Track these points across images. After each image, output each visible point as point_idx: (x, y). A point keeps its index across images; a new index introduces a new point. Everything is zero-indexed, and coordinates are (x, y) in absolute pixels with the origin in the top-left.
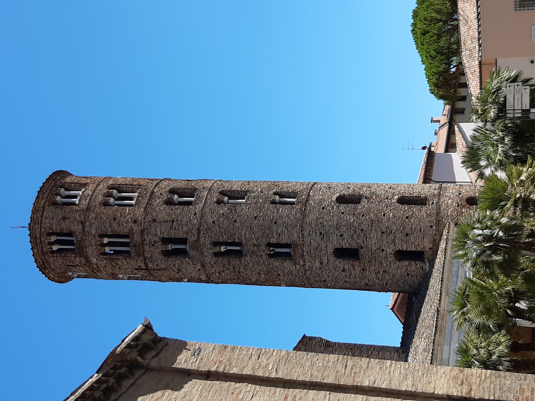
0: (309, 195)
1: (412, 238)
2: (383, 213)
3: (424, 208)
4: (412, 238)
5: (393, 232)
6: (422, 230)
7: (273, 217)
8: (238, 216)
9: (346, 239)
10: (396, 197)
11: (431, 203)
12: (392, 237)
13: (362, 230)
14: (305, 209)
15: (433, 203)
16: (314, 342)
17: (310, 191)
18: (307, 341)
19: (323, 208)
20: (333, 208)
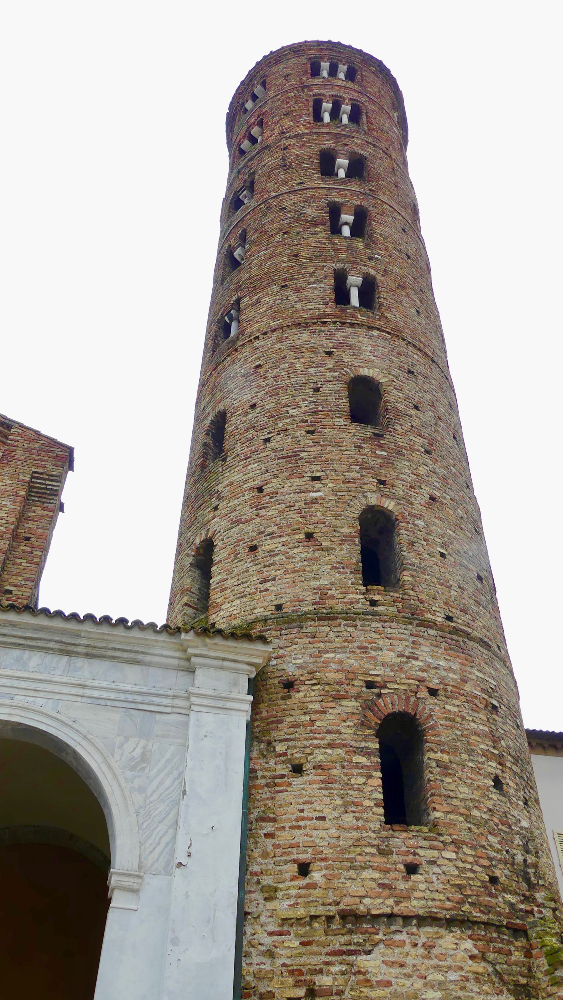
0: (371, 328)
1: (242, 566)
2: (318, 474)
3: (353, 578)
4: (242, 566)
5: (262, 512)
6: (268, 585)
7: (296, 279)
8: (298, 233)
9: (244, 419)
10: (389, 505)
11: (376, 597)
12: (247, 512)
13: (268, 440)
14: (324, 323)
15: (373, 603)
16: (48, 465)
17: (389, 333)
18: (52, 452)
19: (329, 354)
20: (330, 370)
